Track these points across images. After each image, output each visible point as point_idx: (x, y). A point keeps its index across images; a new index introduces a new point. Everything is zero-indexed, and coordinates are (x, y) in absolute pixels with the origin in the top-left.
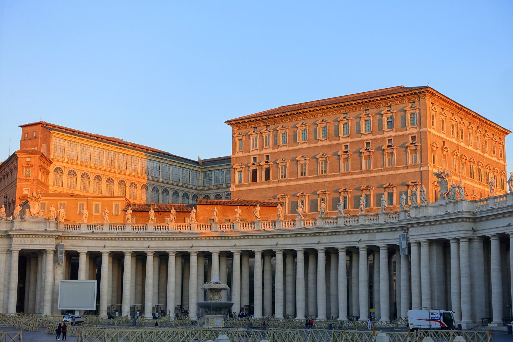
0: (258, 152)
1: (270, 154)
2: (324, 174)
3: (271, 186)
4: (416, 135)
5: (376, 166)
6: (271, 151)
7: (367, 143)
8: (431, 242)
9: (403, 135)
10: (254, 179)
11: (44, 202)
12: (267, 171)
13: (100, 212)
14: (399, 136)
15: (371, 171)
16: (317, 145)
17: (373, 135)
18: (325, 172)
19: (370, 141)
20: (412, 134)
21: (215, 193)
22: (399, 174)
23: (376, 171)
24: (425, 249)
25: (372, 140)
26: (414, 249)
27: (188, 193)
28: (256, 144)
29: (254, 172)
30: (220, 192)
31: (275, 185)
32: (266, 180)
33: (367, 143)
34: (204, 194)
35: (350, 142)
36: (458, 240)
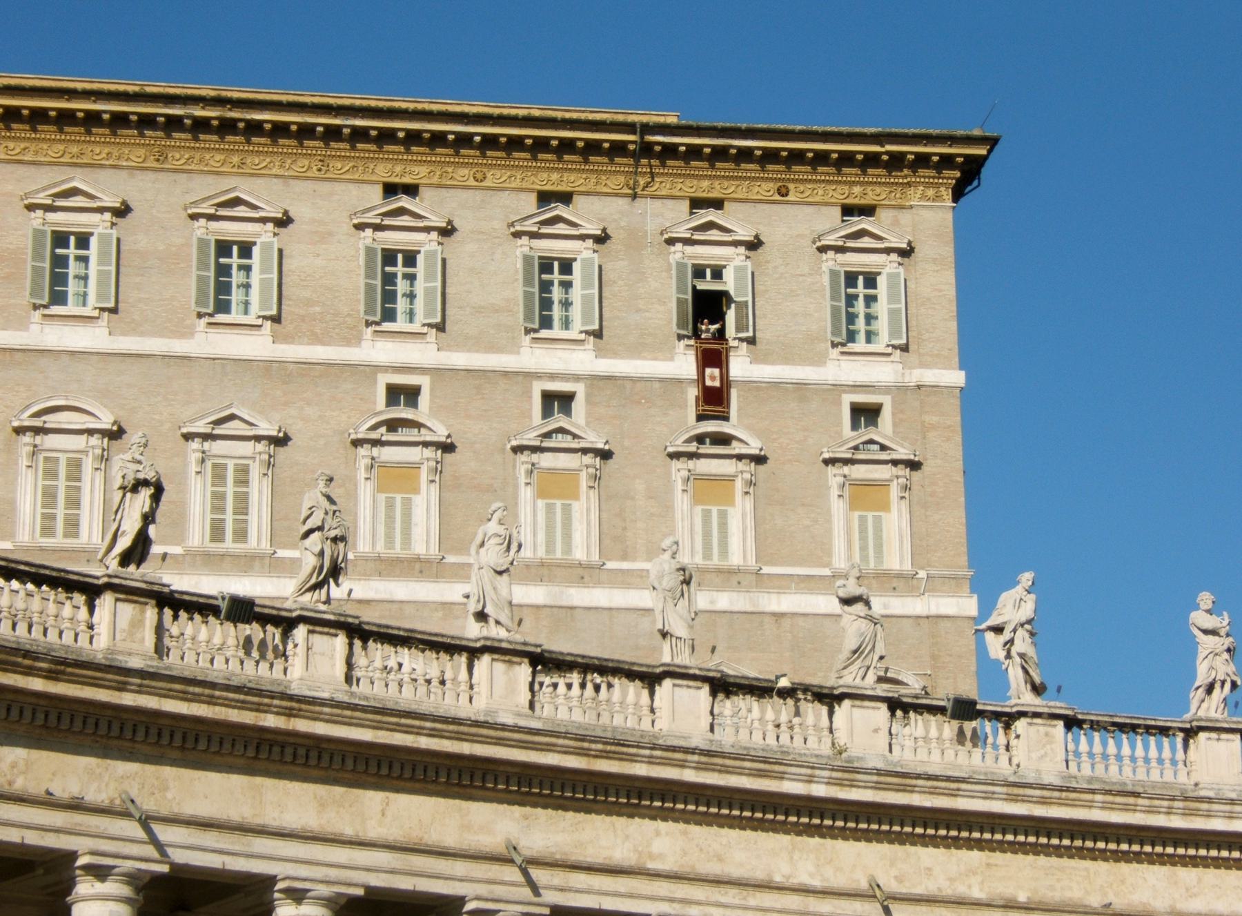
2: (229, 544)
4: (886, 401)
5: (613, 539)
7: (549, 399)
9: (800, 387)
14: (776, 385)
15: (585, 573)
16: (179, 346)
17: (599, 353)
18: (241, 534)
19: (580, 389)
20: (857, 388)
22: (778, 616)
23: (625, 580)
25: (594, 380)
33: (549, 399)
35: (436, 372)
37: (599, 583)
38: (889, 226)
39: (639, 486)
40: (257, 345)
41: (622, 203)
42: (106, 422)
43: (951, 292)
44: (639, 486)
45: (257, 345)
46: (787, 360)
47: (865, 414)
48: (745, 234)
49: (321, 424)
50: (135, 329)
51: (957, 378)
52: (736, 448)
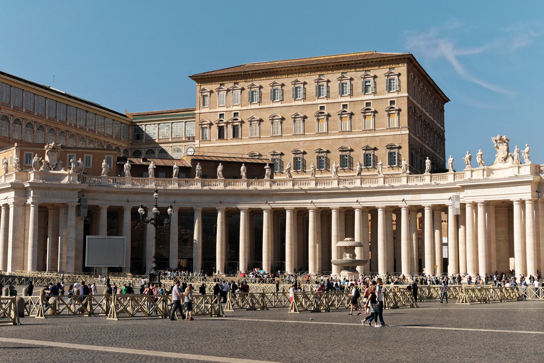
0: (225, 109)
1: (238, 112)
3: (240, 143)
6: (239, 108)
8: (487, 204)
10: (221, 136)
11: (30, 153)
12: (235, 128)
13: (91, 164)
19: (348, 103)
21: (147, 148)
24: (480, 210)
26: (468, 209)
27: (120, 147)
28: (223, 100)
29: (221, 130)
30: (153, 148)
31: (245, 143)
32: (234, 137)
34: (134, 149)
36: (522, 203)
37: (351, 134)
38: (396, 71)
39: (357, 118)
40: (301, 103)
41: (355, 72)
42: (280, 117)
43: (406, 80)
44: (357, 118)
45: (301, 103)
46: (380, 95)
47: (392, 102)
48: (372, 75)
49: (311, 113)
50: (285, 103)
51: (407, 94)
52: (371, 111)
